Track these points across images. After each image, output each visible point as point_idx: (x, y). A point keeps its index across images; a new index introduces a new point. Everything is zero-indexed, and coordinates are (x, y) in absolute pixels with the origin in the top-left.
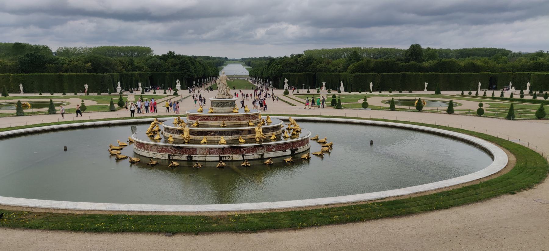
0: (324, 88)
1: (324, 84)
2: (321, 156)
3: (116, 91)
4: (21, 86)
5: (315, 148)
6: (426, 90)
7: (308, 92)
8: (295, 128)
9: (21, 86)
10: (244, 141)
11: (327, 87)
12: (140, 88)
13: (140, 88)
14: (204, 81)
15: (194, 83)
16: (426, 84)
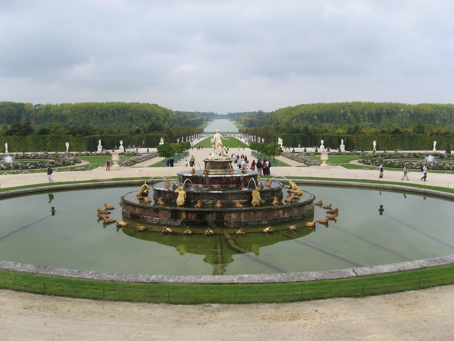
0: (322, 146)
1: (322, 142)
2: (326, 224)
3: (97, 150)
4: (6, 144)
5: (320, 214)
6: (434, 149)
7: (305, 151)
8: (295, 191)
9: (6, 144)
10: (241, 206)
11: (326, 146)
12: (121, 145)
13: (121, 145)
14: (188, 139)
15: (178, 141)
16: (435, 143)
